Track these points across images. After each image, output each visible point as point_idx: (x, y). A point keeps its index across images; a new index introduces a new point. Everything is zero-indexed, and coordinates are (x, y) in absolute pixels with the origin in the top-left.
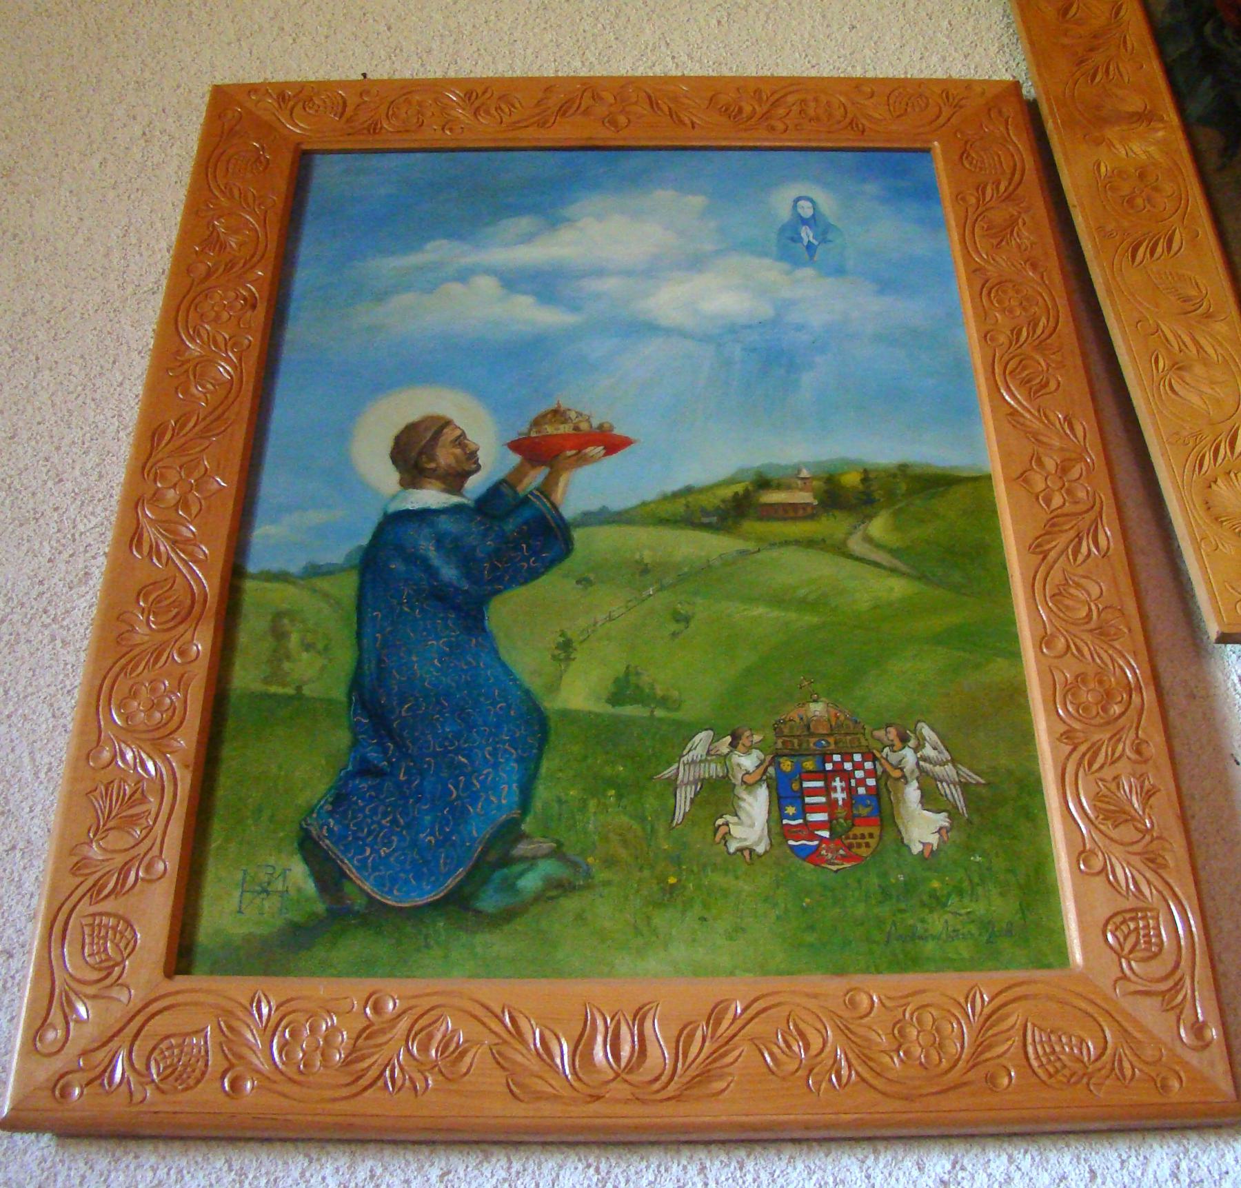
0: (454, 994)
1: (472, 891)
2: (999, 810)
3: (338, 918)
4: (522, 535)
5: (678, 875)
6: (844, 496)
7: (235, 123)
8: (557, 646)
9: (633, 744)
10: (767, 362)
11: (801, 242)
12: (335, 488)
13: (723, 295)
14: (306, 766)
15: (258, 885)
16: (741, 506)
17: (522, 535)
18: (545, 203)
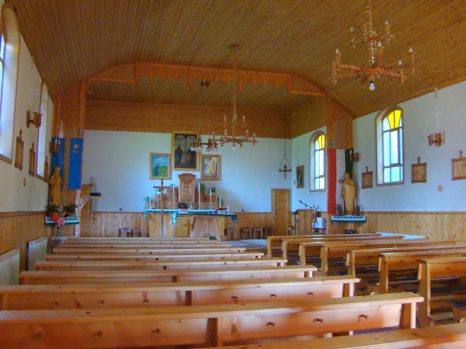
0: (157, 177)
1: (157, 175)
2: (167, 174)
3: (155, 176)
4: (158, 167)
5: (161, 175)
7: (151, 153)
8: (159, 170)
9: (160, 172)
10: (163, 163)
11: (164, 159)
13: (162, 161)
15: (154, 175)
16: (163, 167)
17: (158, 167)
18: (158, 157)
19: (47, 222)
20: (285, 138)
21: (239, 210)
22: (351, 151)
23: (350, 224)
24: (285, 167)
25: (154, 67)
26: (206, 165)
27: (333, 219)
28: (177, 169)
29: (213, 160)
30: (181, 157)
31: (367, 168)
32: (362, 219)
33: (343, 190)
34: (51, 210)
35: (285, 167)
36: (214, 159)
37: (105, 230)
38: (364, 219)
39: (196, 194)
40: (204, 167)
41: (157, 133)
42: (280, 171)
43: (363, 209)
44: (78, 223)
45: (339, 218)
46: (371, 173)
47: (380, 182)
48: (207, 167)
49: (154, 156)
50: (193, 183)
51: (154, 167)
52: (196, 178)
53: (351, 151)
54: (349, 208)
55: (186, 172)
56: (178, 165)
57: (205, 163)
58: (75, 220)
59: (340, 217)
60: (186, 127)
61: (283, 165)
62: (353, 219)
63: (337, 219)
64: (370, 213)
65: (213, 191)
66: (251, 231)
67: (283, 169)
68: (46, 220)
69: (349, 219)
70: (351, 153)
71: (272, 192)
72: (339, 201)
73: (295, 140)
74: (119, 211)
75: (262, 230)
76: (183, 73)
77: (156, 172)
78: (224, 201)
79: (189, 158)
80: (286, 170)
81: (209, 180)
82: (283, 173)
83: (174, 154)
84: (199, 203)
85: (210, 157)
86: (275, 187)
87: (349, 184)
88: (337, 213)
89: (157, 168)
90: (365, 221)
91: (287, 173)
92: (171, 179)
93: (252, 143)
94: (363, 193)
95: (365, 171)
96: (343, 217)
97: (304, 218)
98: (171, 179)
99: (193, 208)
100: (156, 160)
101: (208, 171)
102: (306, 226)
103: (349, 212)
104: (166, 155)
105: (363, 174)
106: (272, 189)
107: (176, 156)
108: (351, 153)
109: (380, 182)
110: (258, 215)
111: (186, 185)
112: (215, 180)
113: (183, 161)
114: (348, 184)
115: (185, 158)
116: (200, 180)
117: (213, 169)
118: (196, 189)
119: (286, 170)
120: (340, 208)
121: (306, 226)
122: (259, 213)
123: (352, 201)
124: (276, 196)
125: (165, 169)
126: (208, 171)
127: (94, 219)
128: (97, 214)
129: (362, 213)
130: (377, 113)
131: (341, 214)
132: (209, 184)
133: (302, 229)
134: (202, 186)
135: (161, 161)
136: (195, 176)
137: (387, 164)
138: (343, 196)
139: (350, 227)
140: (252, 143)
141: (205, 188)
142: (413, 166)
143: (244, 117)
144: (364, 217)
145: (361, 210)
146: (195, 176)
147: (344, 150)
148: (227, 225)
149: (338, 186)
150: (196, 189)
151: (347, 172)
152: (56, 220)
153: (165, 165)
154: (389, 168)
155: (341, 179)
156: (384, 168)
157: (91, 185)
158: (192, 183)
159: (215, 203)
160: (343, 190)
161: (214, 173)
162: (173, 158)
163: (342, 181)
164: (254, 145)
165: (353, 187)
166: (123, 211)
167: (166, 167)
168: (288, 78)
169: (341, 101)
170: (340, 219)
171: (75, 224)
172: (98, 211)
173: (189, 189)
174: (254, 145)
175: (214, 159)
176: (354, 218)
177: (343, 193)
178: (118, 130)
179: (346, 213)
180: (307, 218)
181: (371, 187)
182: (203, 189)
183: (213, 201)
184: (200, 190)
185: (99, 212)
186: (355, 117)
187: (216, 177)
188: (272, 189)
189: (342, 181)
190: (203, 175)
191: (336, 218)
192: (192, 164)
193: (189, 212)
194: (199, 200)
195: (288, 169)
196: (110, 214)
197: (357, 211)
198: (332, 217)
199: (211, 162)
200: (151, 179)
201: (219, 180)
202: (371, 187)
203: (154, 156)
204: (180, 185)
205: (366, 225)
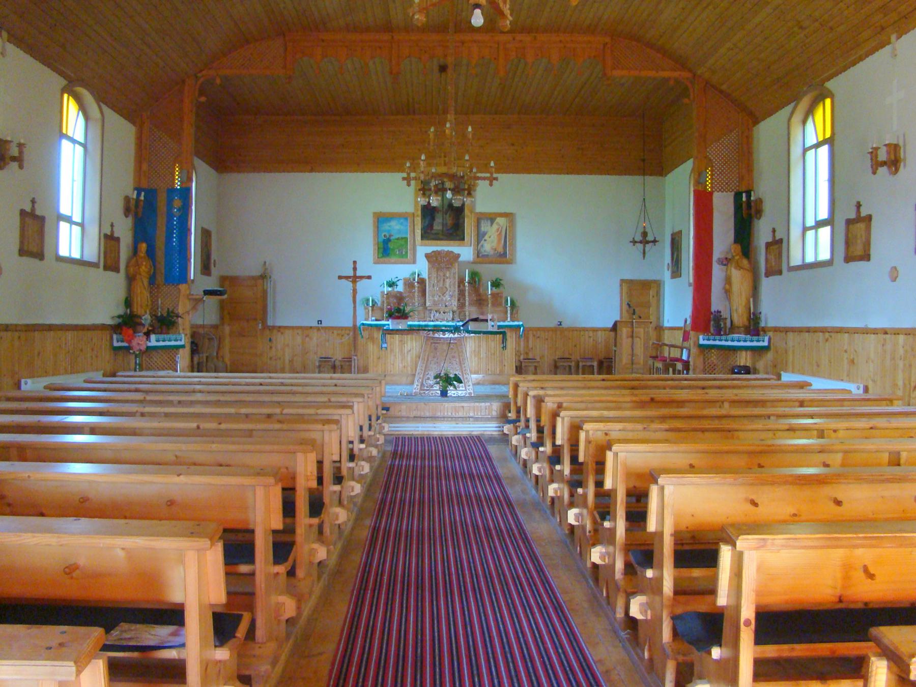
0: (386, 259)
2: (407, 252)
3: (383, 256)
4: (389, 240)
5: (395, 254)
6: (402, 238)
7: (375, 214)
8: (391, 245)
9: (393, 250)
10: (399, 231)
11: (402, 224)
12: (382, 238)
13: (398, 227)
14: (381, 250)
15: (381, 255)
16: (398, 239)
18: (389, 221)
19: (116, 344)
20: (644, 174)
21: (553, 324)
22: (744, 195)
23: (744, 353)
24: (645, 234)
25: (323, 41)
26: (485, 234)
27: (702, 342)
28: (427, 242)
29: (498, 224)
30: (433, 219)
31: (774, 231)
32: (761, 344)
33: (728, 280)
34: (127, 323)
35: (645, 234)
36: (501, 221)
37: (291, 361)
38: (766, 344)
39: (462, 293)
40: (480, 236)
41: (386, 174)
42: (634, 242)
43: (766, 323)
44: (183, 347)
45: (714, 340)
46: (781, 241)
47: (796, 260)
48: (486, 237)
49: (380, 219)
50: (455, 270)
51: (381, 240)
52: (461, 259)
53: (744, 195)
54: (740, 318)
55: (439, 249)
56: (428, 234)
57: (483, 229)
58: (176, 340)
59: (717, 337)
60: (443, 159)
61: (641, 230)
62: (748, 344)
63: (711, 342)
64: (776, 330)
65: (496, 284)
66: (573, 364)
67: (638, 238)
68: (115, 341)
69: (742, 344)
70: (744, 199)
71: (621, 285)
72: (717, 303)
73: (670, 176)
74: (315, 324)
75: (595, 364)
76: (380, 48)
77: (386, 249)
78: (517, 304)
79: (449, 221)
80: (645, 240)
81: (491, 263)
82: (640, 246)
83: (419, 213)
84: (467, 308)
85: (492, 218)
86: (628, 276)
87: (739, 267)
88: (712, 329)
89: (387, 241)
90: (766, 349)
91: (648, 246)
92: (414, 262)
93: (487, 182)
94: (766, 284)
95: (770, 240)
96: (724, 337)
97: (630, 339)
98: (414, 262)
99: (453, 319)
100: (386, 227)
101: (489, 246)
102: (633, 355)
103: (738, 327)
104: (403, 216)
105: (768, 245)
106: (622, 281)
107: (424, 216)
108: (744, 199)
109: (796, 260)
110: (591, 334)
111: (442, 274)
112: (500, 263)
113: (437, 226)
114: (736, 268)
115: (445, 221)
116: (474, 263)
117: (499, 240)
118: (461, 281)
119: (645, 240)
120: (718, 317)
121: (633, 355)
122: (595, 330)
123: (744, 304)
124: (630, 295)
125: (402, 242)
126: (489, 246)
127: (270, 340)
128: (275, 331)
129: (765, 330)
130: (789, 108)
131: (718, 332)
132: (488, 272)
133: (624, 361)
134: (474, 275)
135: (395, 228)
136: (459, 256)
137: (810, 222)
138: (728, 292)
139: (744, 359)
140: (487, 182)
141: (479, 280)
142: (849, 222)
143: (470, 129)
144: (766, 339)
145: (762, 324)
146: (459, 256)
147: (733, 193)
148: (527, 353)
149: (718, 273)
150: (461, 281)
151: (736, 241)
152: (129, 342)
153: (404, 236)
154: (813, 231)
155: (723, 256)
156: (805, 229)
157: (263, 277)
158: (453, 271)
159: (500, 308)
160: (728, 280)
161: (501, 250)
162: (418, 220)
163: (726, 262)
164: (491, 185)
165: (748, 276)
166: (324, 325)
167: (406, 239)
168: (605, 45)
169: (724, 87)
170: (717, 343)
171: (178, 348)
172: (278, 324)
173: (448, 281)
174: (491, 185)
175: (501, 221)
176: (745, 341)
177: (727, 286)
178: (312, 170)
179: (733, 329)
180: (637, 340)
181: (780, 272)
182: (475, 282)
183: (494, 305)
184: (469, 283)
185: (280, 327)
186: (756, 121)
187: (504, 256)
188: (622, 281)
189: (726, 262)
190: (478, 254)
191: (708, 340)
192: (455, 232)
193: (410, 326)
194: (467, 303)
195: (650, 238)
196: (300, 331)
197: (754, 327)
198: (701, 337)
199: (495, 226)
200: (375, 263)
201: (510, 262)
202: (780, 272)
203: (380, 219)
204: (429, 274)
205: (770, 355)
